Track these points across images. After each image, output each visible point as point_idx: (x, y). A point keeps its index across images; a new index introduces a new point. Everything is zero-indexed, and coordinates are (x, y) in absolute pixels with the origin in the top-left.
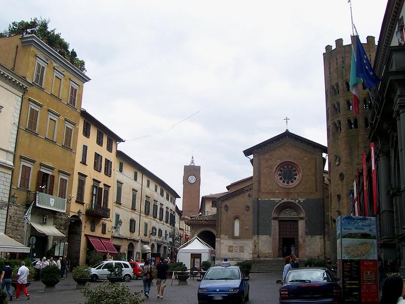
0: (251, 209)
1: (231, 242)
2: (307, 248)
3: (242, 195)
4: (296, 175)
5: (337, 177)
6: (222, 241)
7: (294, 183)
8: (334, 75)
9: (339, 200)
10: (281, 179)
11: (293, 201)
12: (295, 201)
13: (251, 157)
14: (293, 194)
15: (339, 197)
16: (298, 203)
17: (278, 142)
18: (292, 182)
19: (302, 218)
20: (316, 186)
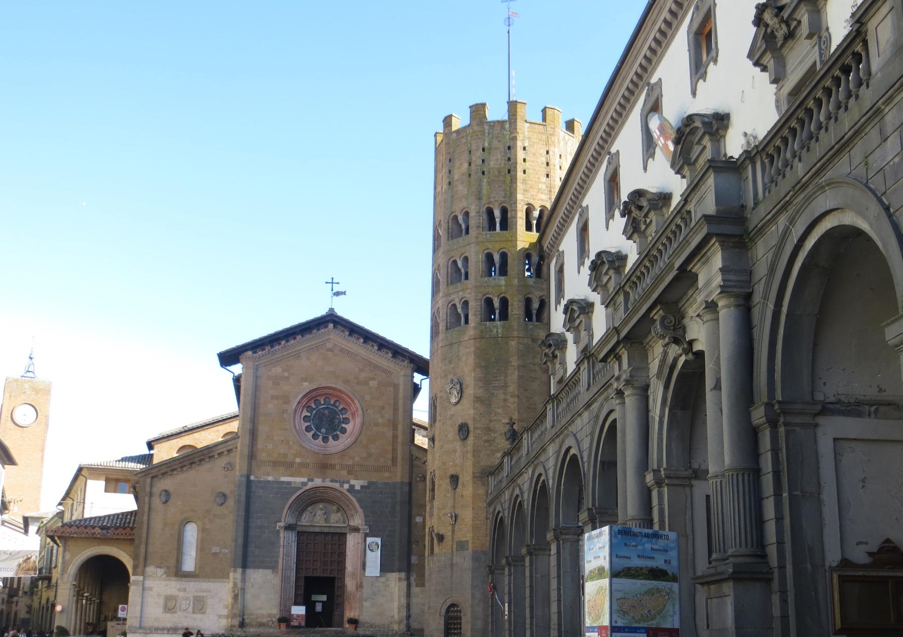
0: (231, 502)
1: (172, 587)
2: (366, 604)
4: (346, 421)
5: (452, 433)
6: (148, 583)
7: (341, 440)
8: (460, 188)
9: (455, 489)
10: (308, 429)
11: (336, 485)
12: (342, 486)
13: (237, 369)
14: (338, 467)
15: (455, 479)
16: (348, 490)
17: (308, 336)
18: (336, 438)
19: (356, 530)
20: (394, 450)
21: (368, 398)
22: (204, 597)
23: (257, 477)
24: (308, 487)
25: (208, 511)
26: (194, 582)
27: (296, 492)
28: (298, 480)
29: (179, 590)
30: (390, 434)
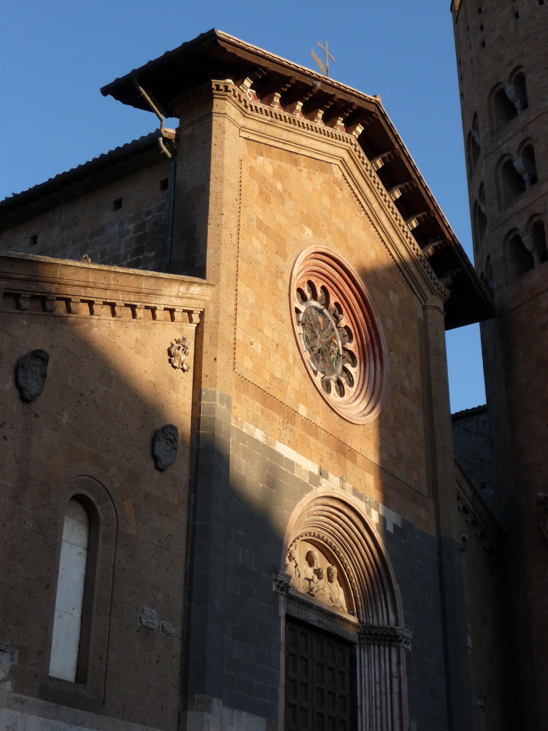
21: (389, 323)
30: (420, 421)
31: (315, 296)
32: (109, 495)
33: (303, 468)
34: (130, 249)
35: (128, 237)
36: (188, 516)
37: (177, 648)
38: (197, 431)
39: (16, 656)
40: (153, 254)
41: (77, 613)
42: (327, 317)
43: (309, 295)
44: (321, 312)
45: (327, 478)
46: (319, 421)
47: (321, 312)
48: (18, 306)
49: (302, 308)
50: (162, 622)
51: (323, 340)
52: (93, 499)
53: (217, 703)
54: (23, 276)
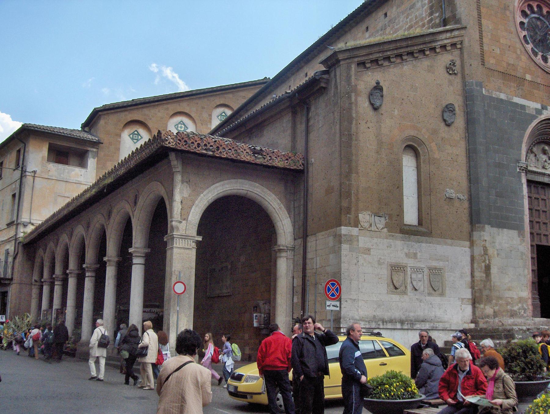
3: (425, 63)
22: (440, 269)
23: (488, 91)
24: (543, 117)
25: (435, 132)
26: (427, 242)
27: (531, 121)
28: (533, 105)
29: (407, 255)
31: (533, 12)
32: (423, 142)
33: (531, 107)
34: (427, 13)
35: (425, 7)
36: (466, 144)
37: (466, 205)
38: (466, 103)
39: (387, 218)
40: (437, 14)
41: (416, 196)
42: (542, 20)
43: (529, 12)
44: (538, 19)
45: (547, 109)
46: (539, 80)
47: (538, 19)
48: (365, 67)
49: (526, 21)
50: (457, 194)
51: (541, 34)
52: (416, 145)
53: (487, 227)
54: (364, 54)
